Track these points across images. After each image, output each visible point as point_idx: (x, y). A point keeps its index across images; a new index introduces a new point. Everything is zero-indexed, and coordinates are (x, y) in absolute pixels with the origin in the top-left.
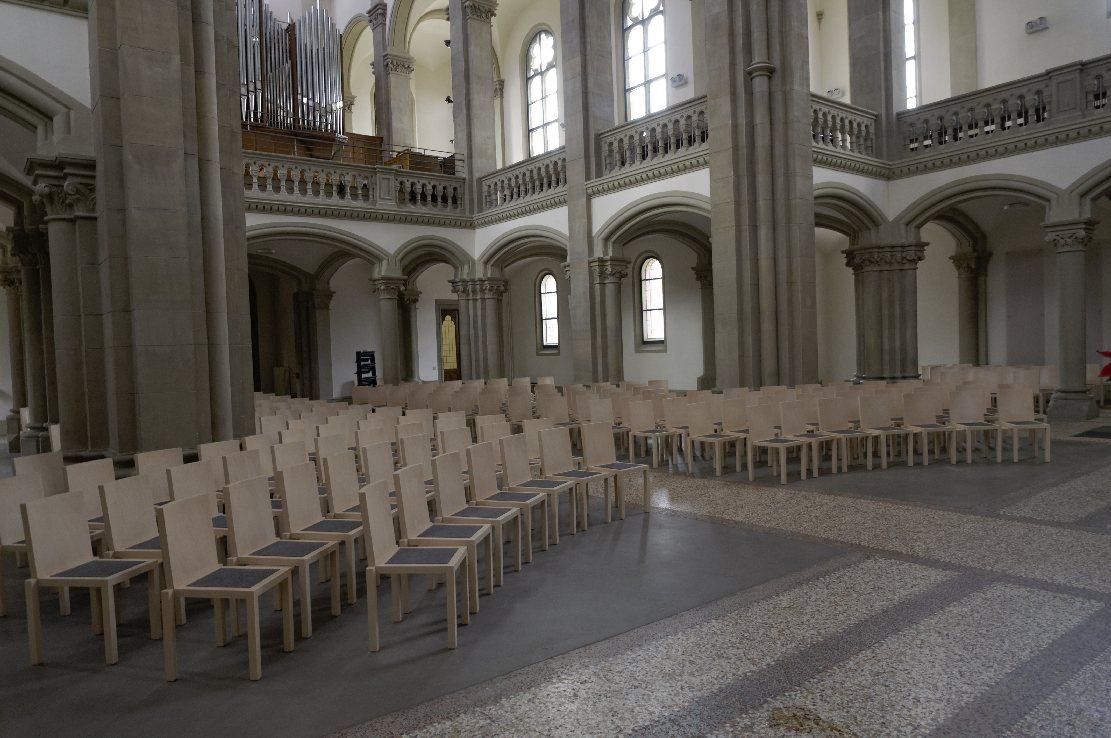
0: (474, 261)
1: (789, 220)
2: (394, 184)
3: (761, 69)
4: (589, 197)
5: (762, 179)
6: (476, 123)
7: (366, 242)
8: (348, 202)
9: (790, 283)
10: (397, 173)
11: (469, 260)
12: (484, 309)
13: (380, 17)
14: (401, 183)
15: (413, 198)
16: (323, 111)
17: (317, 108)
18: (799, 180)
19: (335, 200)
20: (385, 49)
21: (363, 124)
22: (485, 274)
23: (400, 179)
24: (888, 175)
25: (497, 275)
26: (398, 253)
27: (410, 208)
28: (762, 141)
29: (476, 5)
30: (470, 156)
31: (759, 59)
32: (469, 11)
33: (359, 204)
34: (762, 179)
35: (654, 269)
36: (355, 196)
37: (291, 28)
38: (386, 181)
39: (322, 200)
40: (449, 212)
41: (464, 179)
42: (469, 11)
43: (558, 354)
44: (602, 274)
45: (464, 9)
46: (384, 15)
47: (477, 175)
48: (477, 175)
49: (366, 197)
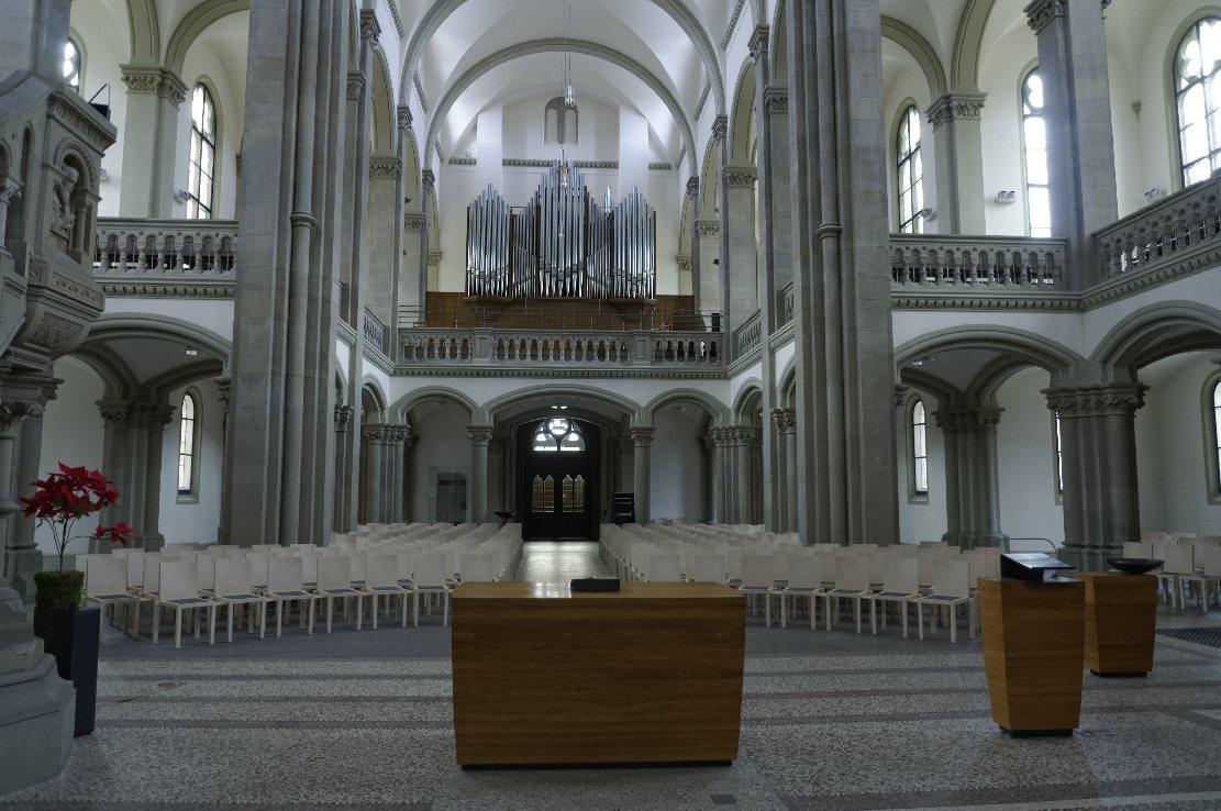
0: (729, 410)
1: (854, 377)
2: (650, 346)
3: (827, 231)
4: (772, 352)
5: (829, 337)
6: (733, 282)
7: (621, 397)
8: (608, 365)
9: (856, 439)
10: (653, 335)
11: (724, 409)
12: (736, 455)
15: (670, 356)
17: (629, 278)
18: (863, 337)
19: (596, 364)
20: (697, 216)
21: (669, 284)
22: (736, 421)
24: (1080, 307)
25: (747, 422)
26: (649, 406)
27: (666, 365)
28: (828, 300)
30: (727, 313)
31: (827, 220)
33: (618, 365)
34: (829, 337)
35: (919, 406)
36: (602, 356)
37: (612, 215)
39: (583, 364)
40: (706, 366)
43: (926, 503)
44: (780, 425)
45: (725, 180)
46: (696, 187)
47: (733, 329)
48: (733, 329)
49: (624, 358)
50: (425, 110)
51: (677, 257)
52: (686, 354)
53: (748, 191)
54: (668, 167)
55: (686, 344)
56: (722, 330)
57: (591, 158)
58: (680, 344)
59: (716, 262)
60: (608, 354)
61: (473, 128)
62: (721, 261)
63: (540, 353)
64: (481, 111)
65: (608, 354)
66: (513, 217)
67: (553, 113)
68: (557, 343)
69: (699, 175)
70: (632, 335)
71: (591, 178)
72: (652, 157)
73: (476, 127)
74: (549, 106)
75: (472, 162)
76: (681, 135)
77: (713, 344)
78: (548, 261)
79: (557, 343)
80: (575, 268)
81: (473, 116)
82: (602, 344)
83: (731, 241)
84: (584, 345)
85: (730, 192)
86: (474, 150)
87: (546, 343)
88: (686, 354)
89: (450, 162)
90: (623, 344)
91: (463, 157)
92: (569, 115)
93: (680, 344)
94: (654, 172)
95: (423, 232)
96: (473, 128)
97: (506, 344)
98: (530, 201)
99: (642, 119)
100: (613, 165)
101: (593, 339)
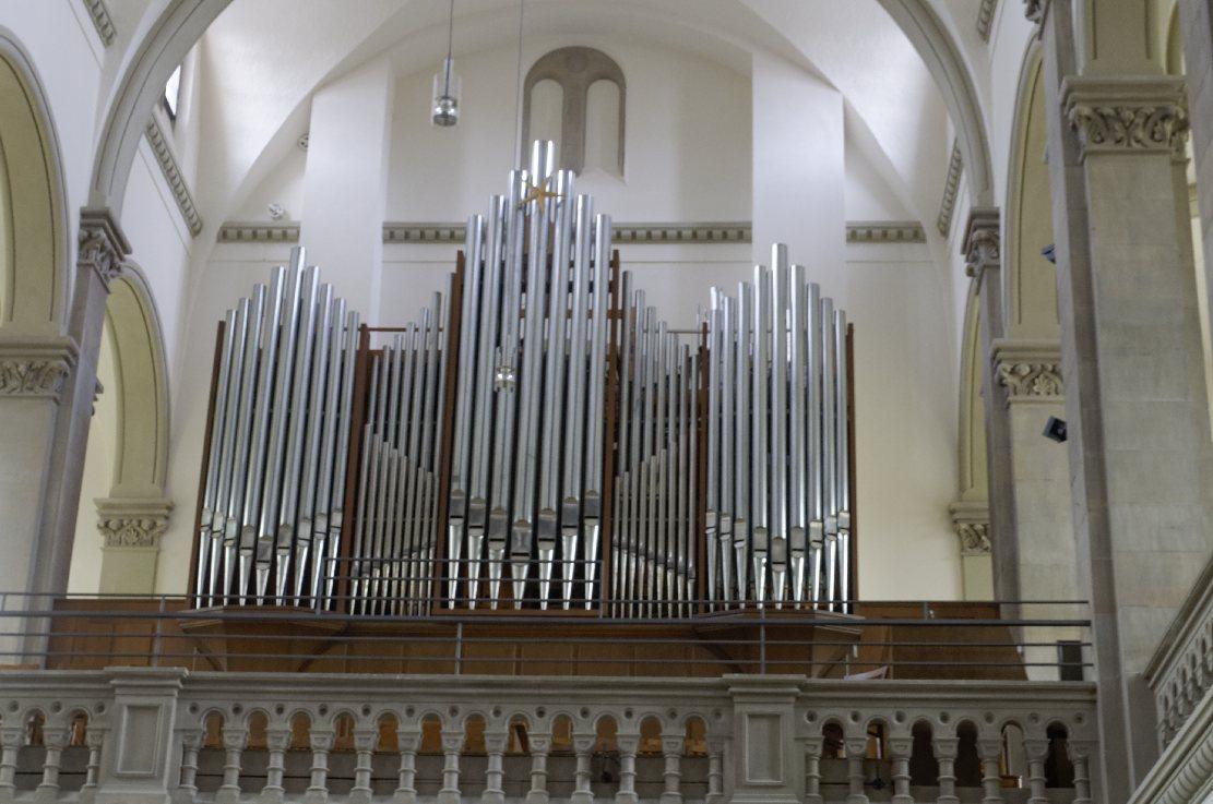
2: (797, 732)
6: (1120, 485)
13: (983, 252)
14: (833, 732)
16: (778, 551)
17: (760, 540)
20: (996, 329)
23: (825, 714)
29: (1108, 110)
32: (1083, 134)
38: (764, 725)
41: (1093, 690)
42: (1083, 134)
45: (1070, 130)
46: (992, 242)
48: (1132, 667)
50: (108, 40)
51: (952, 512)
52: (947, 771)
53: (1154, 170)
54: (908, 233)
55: (945, 736)
56: (1092, 676)
57: (663, 213)
58: (922, 733)
59: (1057, 430)
60: (630, 766)
61: (297, 139)
62: (1074, 427)
63: (365, 764)
64: (324, 85)
65: (630, 766)
66: (366, 358)
67: (549, 96)
68: (432, 727)
69: (1000, 200)
70: (725, 697)
71: (651, 273)
72: (862, 208)
73: (306, 135)
74: (539, 72)
75: (287, 235)
76: (949, 120)
77: (1057, 733)
78: (479, 490)
79: (432, 727)
80: (571, 506)
81: (305, 93)
82: (607, 725)
83: (1103, 339)
84: (541, 737)
85: (1093, 168)
86: (298, 202)
87: (388, 723)
88: (947, 771)
89: (224, 236)
90: (693, 727)
91: (264, 218)
92: (600, 96)
93: (922, 733)
94: (863, 251)
95: (62, 401)
96: (297, 139)
97: (236, 734)
98: (430, 304)
99: (822, 90)
100: (739, 234)
101: (575, 712)
